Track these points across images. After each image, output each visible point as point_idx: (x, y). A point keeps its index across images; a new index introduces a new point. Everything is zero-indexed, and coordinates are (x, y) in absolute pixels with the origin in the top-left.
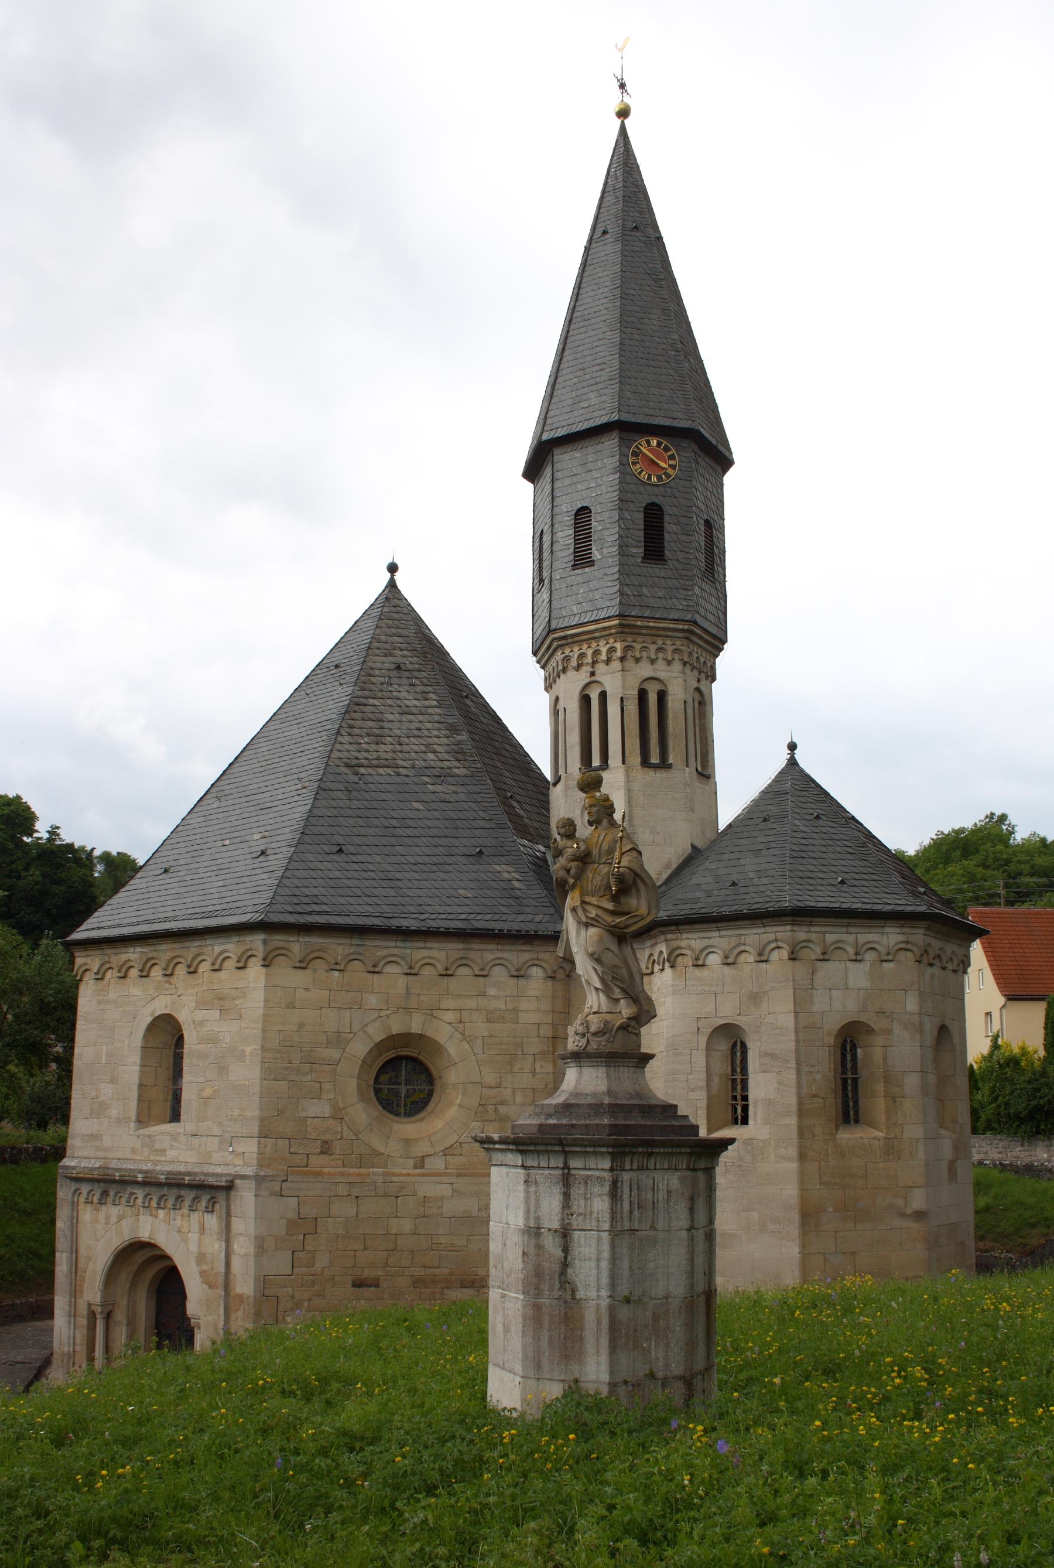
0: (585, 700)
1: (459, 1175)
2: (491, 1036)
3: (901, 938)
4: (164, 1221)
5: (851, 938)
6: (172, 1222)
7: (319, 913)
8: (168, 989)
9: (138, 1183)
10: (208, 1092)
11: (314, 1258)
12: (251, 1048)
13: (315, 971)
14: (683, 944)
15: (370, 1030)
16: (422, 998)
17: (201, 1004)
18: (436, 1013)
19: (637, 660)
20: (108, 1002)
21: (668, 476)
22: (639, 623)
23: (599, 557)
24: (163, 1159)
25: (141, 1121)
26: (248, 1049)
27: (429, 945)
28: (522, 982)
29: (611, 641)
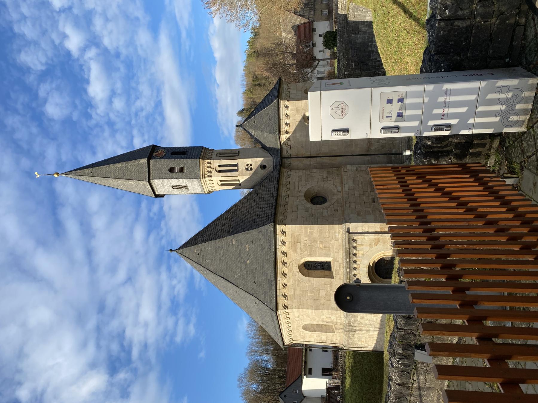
0: (220, 171)
1: (342, 184)
2: (305, 180)
3: (285, 85)
4: (361, 261)
5: (284, 92)
6: (361, 258)
7: (271, 212)
8: (291, 266)
9: (350, 271)
10: (321, 246)
11: (367, 211)
12: (309, 228)
13: (287, 215)
14: (284, 130)
15: (303, 203)
16: (295, 193)
17: (295, 251)
18: (299, 190)
19: (211, 157)
20: (295, 294)
21: (164, 151)
22: (202, 156)
23: (183, 165)
24: (342, 265)
25: (332, 277)
26: (309, 230)
27: (281, 191)
28: (291, 175)
29: (205, 162)
